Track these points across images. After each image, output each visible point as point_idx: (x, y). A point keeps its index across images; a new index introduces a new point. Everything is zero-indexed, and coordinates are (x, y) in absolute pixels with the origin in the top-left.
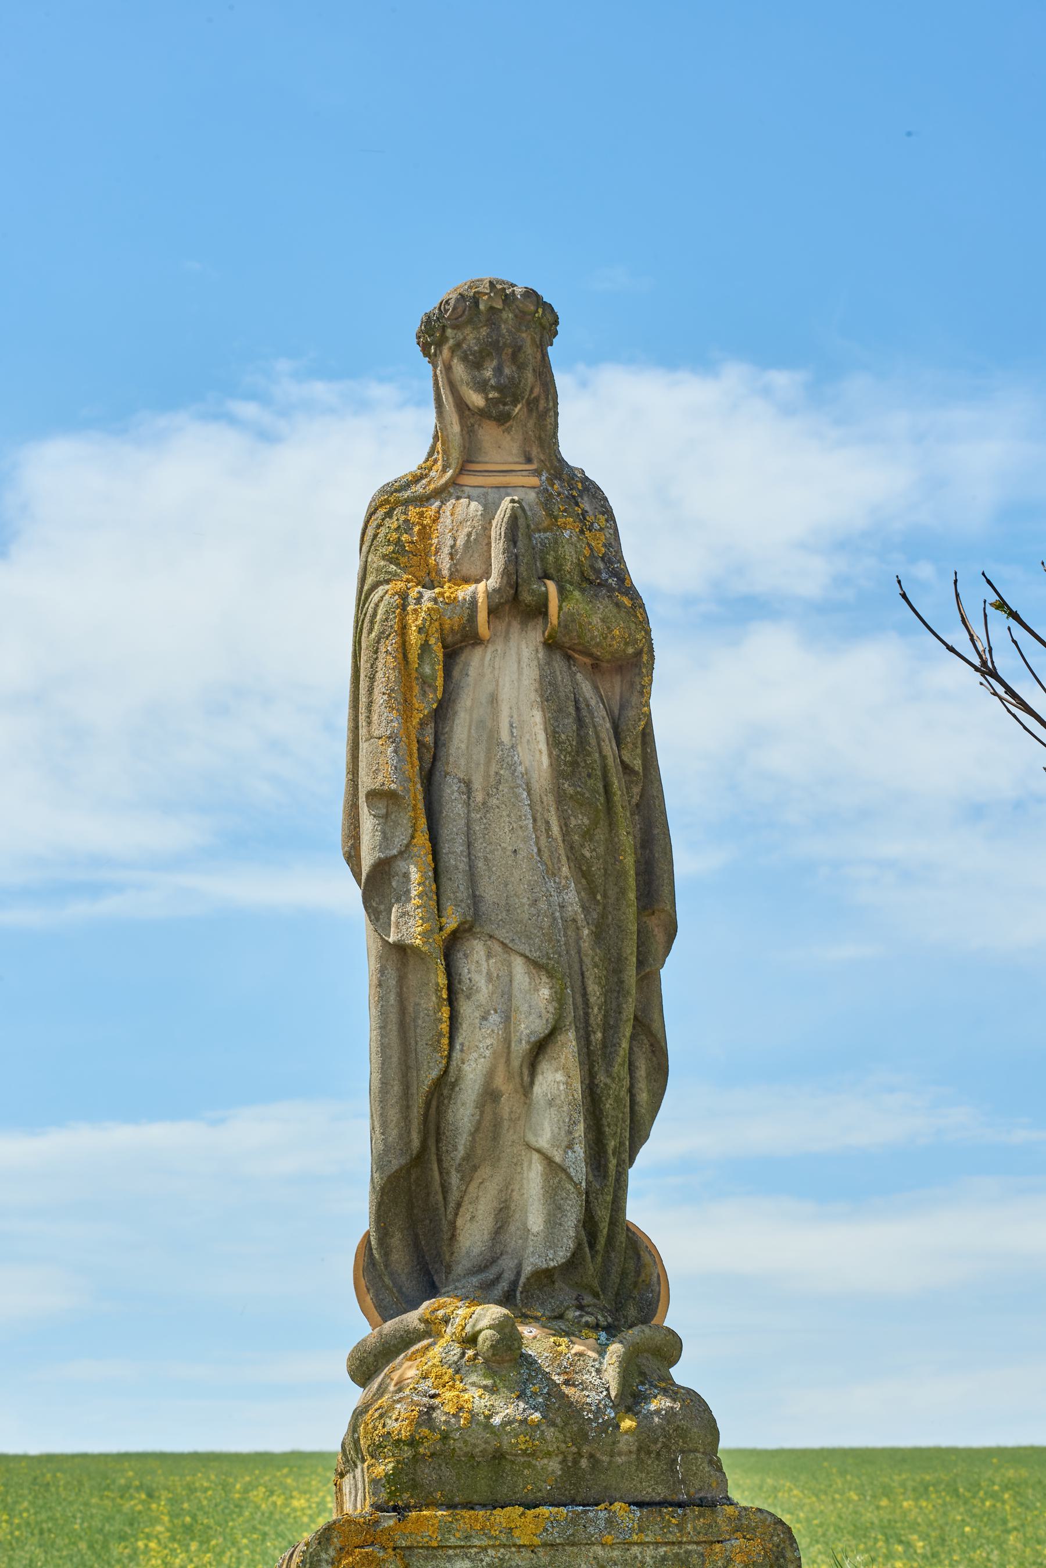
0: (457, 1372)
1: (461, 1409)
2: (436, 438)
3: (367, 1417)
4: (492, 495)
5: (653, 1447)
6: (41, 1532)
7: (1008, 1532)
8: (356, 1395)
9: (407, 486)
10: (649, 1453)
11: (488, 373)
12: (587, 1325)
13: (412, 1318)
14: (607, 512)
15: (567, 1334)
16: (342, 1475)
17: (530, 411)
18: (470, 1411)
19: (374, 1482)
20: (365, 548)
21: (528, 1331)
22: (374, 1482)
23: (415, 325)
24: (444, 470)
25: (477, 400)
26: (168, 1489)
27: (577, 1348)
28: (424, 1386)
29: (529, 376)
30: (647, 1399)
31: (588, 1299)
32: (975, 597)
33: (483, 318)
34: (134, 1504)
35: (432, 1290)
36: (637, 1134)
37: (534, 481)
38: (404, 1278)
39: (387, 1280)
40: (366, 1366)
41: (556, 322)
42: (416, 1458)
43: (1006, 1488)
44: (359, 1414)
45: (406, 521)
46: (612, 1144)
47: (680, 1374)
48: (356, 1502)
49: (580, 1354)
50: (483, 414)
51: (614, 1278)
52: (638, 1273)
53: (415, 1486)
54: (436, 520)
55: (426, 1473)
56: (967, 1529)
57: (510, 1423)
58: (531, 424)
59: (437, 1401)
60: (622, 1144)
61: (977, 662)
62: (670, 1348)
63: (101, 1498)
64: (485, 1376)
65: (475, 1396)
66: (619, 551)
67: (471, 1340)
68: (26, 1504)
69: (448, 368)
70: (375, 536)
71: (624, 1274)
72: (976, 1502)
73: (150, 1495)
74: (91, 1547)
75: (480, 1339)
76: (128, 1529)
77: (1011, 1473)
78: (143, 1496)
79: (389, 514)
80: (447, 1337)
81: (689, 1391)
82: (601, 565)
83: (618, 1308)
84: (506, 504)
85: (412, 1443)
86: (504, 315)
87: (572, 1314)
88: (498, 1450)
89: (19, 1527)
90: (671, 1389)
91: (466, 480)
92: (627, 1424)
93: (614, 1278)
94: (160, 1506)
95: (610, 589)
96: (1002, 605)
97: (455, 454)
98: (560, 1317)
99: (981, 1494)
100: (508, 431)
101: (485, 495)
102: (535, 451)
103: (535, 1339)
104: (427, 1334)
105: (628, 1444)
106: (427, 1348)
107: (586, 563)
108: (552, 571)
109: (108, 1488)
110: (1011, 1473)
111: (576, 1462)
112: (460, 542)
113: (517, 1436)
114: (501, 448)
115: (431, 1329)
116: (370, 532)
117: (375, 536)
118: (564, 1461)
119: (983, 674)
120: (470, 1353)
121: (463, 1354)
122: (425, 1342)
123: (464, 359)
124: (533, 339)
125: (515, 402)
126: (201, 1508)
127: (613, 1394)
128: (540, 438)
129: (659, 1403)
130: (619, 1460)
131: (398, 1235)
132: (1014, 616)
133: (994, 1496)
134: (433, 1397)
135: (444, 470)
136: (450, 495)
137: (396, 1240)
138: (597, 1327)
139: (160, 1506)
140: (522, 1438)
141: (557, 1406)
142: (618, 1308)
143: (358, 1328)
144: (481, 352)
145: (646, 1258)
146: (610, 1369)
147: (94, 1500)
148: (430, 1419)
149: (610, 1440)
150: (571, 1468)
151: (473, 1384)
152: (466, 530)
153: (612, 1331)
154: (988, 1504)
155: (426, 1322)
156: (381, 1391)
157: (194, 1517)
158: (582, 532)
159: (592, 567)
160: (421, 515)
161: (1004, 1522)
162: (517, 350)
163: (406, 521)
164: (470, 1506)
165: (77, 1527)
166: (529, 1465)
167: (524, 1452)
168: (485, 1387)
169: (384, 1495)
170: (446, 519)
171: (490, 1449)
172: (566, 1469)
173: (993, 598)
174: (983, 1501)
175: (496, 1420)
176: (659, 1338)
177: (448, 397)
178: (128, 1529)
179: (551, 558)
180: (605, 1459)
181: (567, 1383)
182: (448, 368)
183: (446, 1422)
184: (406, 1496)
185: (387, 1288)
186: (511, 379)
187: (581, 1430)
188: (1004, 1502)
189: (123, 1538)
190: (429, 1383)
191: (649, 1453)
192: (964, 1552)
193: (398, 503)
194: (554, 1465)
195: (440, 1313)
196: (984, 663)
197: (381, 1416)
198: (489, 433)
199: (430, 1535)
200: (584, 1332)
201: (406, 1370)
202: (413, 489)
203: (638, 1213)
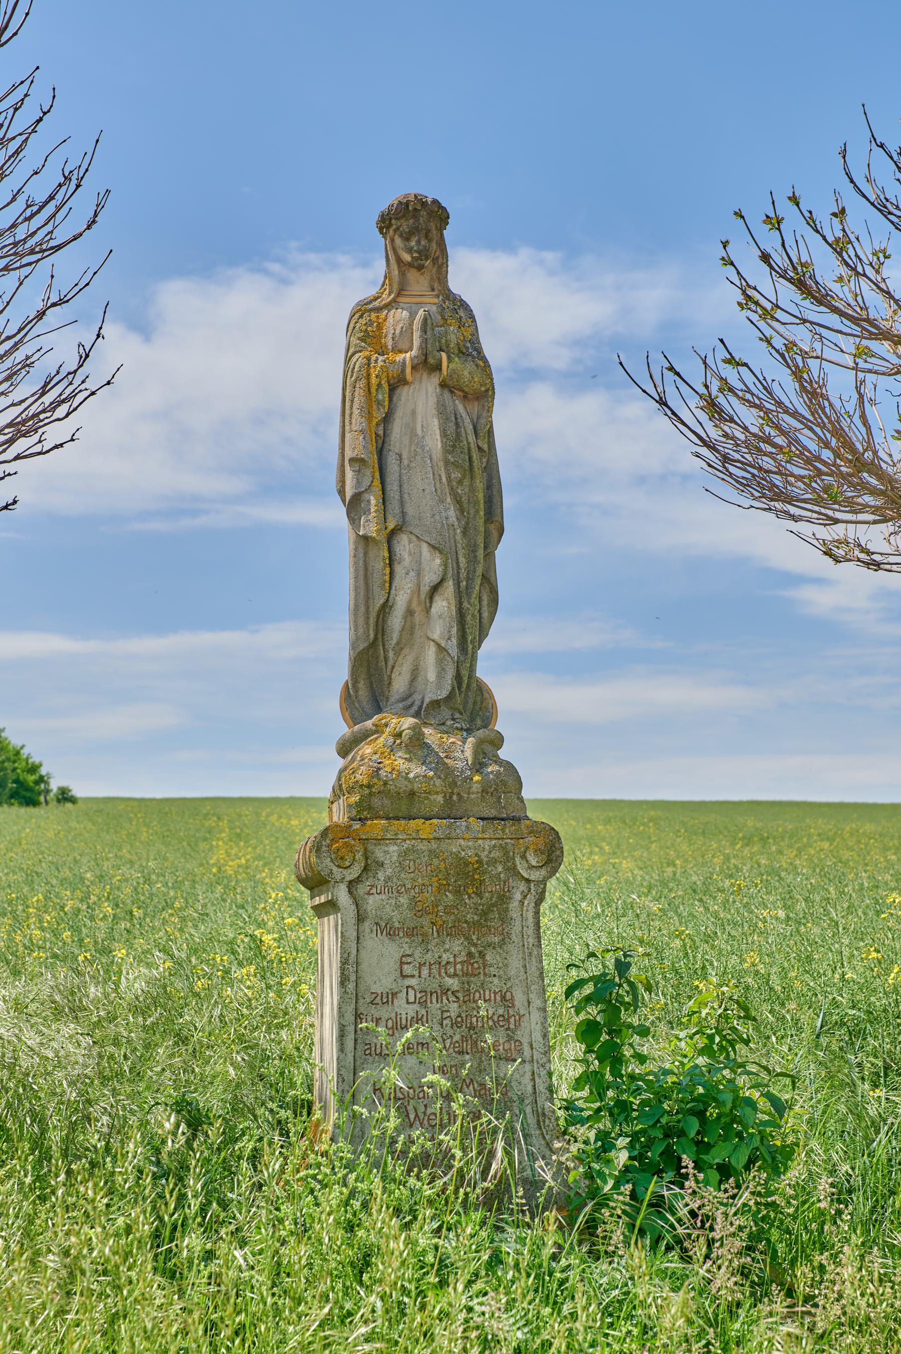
0: (392, 751)
1: (393, 769)
2: (386, 277)
3: (346, 773)
4: (414, 307)
5: (490, 790)
6: (164, 837)
7: (652, 842)
8: (341, 762)
9: (371, 302)
10: (487, 793)
11: (413, 243)
12: (457, 728)
13: (369, 724)
14: (473, 318)
15: (447, 733)
16: (332, 803)
17: (434, 264)
18: (398, 771)
19: (349, 806)
20: (349, 334)
21: (427, 731)
22: (349, 806)
23: (376, 217)
24: (390, 294)
25: (407, 257)
26: (228, 815)
27: (452, 740)
28: (375, 757)
29: (434, 245)
30: (486, 765)
31: (457, 715)
32: (657, 364)
33: (411, 214)
34: (211, 822)
35: (379, 710)
36: (483, 633)
37: (436, 300)
38: (365, 703)
39: (357, 705)
40: (345, 749)
41: (448, 218)
42: (371, 794)
43: (650, 820)
44: (341, 771)
45: (370, 320)
46: (470, 638)
47: (502, 754)
48: (340, 815)
49: (454, 743)
50: (410, 265)
51: (470, 705)
52: (482, 703)
53: (370, 808)
54: (385, 320)
55: (376, 802)
56: (631, 841)
57: (418, 777)
58: (434, 271)
59: (381, 765)
60: (475, 638)
61: (657, 398)
62: (498, 741)
63: (194, 820)
64: (406, 753)
65: (400, 763)
66: (478, 338)
67: (399, 735)
68: (155, 823)
69: (392, 240)
70: (354, 328)
71: (475, 703)
72: (635, 827)
73: (219, 818)
74: (189, 845)
75: (403, 734)
76: (208, 836)
77: (652, 813)
78: (215, 819)
79: (361, 317)
80: (387, 733)
81: (508, 762)
82: (469, 345)
83: (472, 720)
84: (421, 312)
85: (369, 786)
86: (422, 213)
87: (449, 723)
88: (411, 790)
89: (152, 835)
90: (499, 761)
91: (401, 299)
92: (477, 778)
93: (470, 705)
94: (224, 824)
95: (474, 357)
96: (671, 369)
97: (396, 287)
98: (444, 724)
99: (638, 823)
100: (422, 274)
101: (411, 307)
102: (436, 285)
103: (431, 735)
104: (376, 732)
105: (477, 788)
106: (376, 739)
107: (461, 344)
108: (444, 347)
109: (197, 815)
110: (652, 813)
111: (451, 797)
112: (398, 332)
113: (421, 783)
114: (419, 283)
115: (378, 730)
116: (351, 326)
117: (354, 328)
118: (445, 796)
119: (660, 404)
120: (398, 741)
121: (395, 742)
122: (375, 736)
123: (401, 236)
124: (436, 226)
125: (427, 259)
126: (245, 825)
127: (470, 763)
128: (439, 279)
129: (492, 768)
130: (472, 796)
131: (362, 682)
132: (678, 374)
133: (644, 824)
134: (379, 763)
135: (390, 294)
136: (393, 307)
137: (361, 685)
138: (462, 729)
139: (224, 824)
140: (424, 785)
141: (442, 768)
142: (472, 720)
143: (342, 729)
144: (409, 232)
145: (486, 695)
146: (468, 751)
147: (191, 821)
148: (378, 774)
149: (468, 786)
150: (448, 800)
151: (400, 757)
152: (401, 325)
153: (469, 731)
154: (641, 828)
155: (376, 726)
156: (353, 760)
157: (242, 830)
158: (459, 327)
159: (464, 346)
160: (378, 317)
161: (650, 837)
162: (428, 232)
163: (370, 320)
164: (397, 818)
165: (182, 834)
166: (428, 798)
167: (425, 792)
168: (406, 759)
169: (354, 813)
170: (390, 320)
171: (408, 790)
172: (446, 801)
173: (668, 365)
174: (639, 827)
175: (411, 775)
176: (493, 735)
177: (393, 256)
178: (208, 836)
179: (443, 341)
180: (466, 796)
181: (446, 757)
182: (392, 240)
183: (386, 776)
184: (365, 813)
185: (357, 708)
186: (425, 247)
187: (453, 780)
188: (649, 828)
189: (205, 839)
190: (377, 756)
191: (487, 793)
192: (630, 852)
193: (366, 311)
194: (440, 799)
195: (383, 721)
196: (661, 398)
197: (353, 773)
198: (412, 275)
199: (377, 833)
200: (456, 731)
201: (367, 749)
202: (374, 303)
203: (481, 673)
